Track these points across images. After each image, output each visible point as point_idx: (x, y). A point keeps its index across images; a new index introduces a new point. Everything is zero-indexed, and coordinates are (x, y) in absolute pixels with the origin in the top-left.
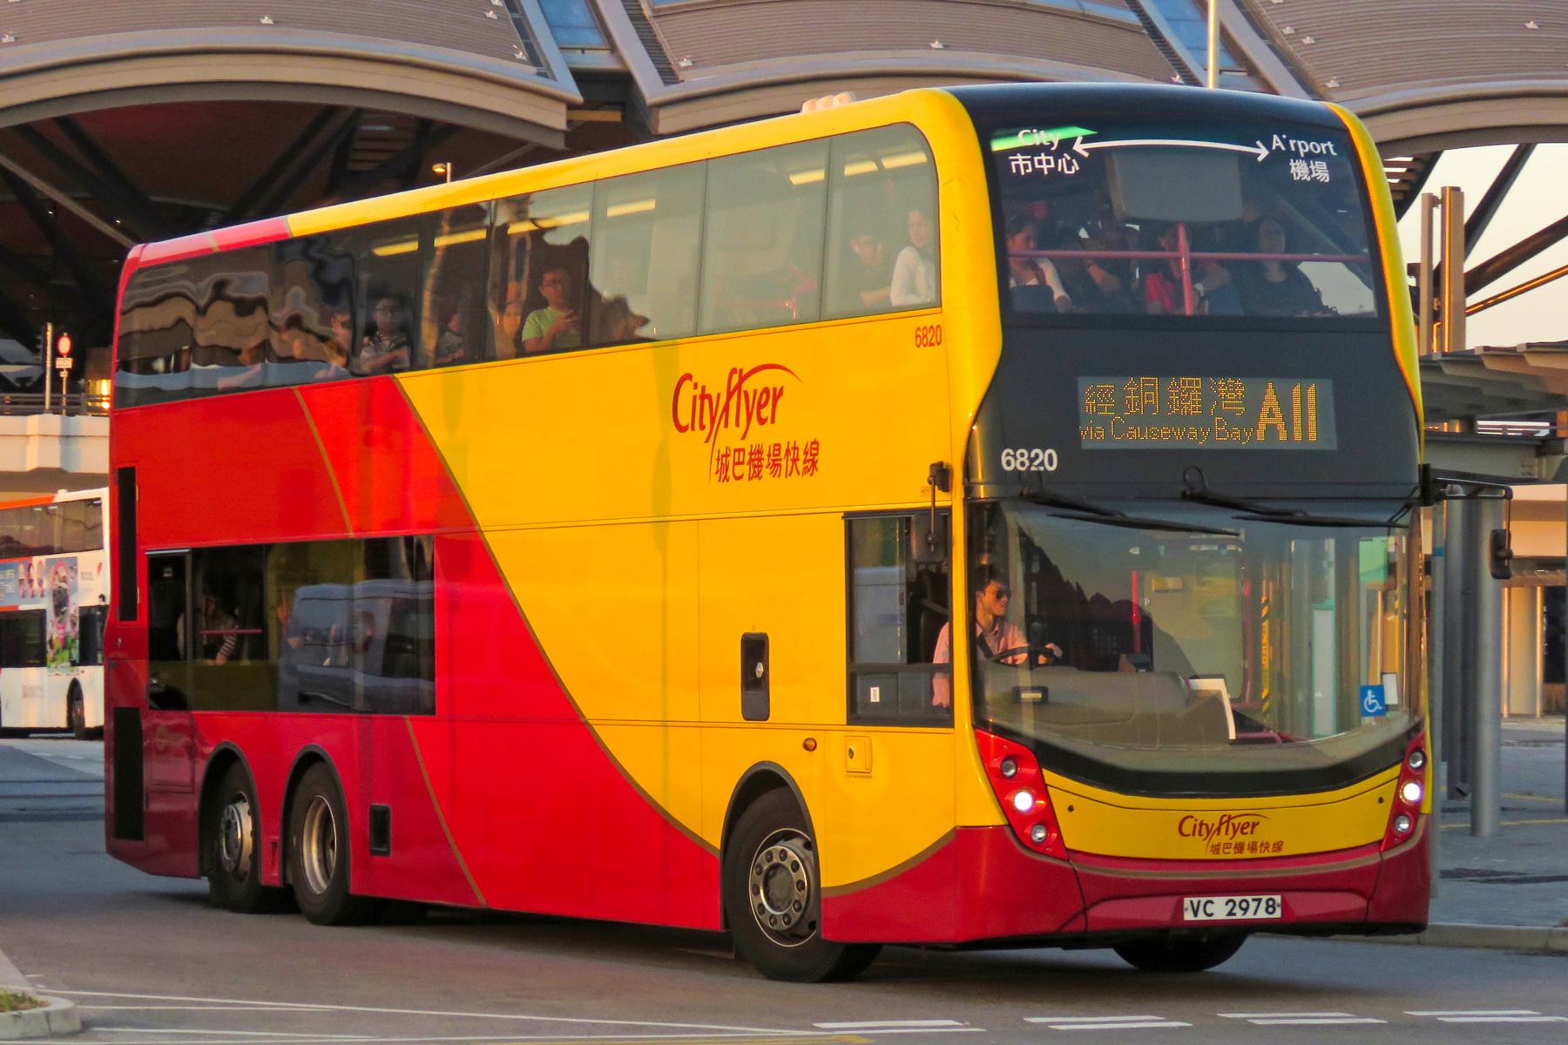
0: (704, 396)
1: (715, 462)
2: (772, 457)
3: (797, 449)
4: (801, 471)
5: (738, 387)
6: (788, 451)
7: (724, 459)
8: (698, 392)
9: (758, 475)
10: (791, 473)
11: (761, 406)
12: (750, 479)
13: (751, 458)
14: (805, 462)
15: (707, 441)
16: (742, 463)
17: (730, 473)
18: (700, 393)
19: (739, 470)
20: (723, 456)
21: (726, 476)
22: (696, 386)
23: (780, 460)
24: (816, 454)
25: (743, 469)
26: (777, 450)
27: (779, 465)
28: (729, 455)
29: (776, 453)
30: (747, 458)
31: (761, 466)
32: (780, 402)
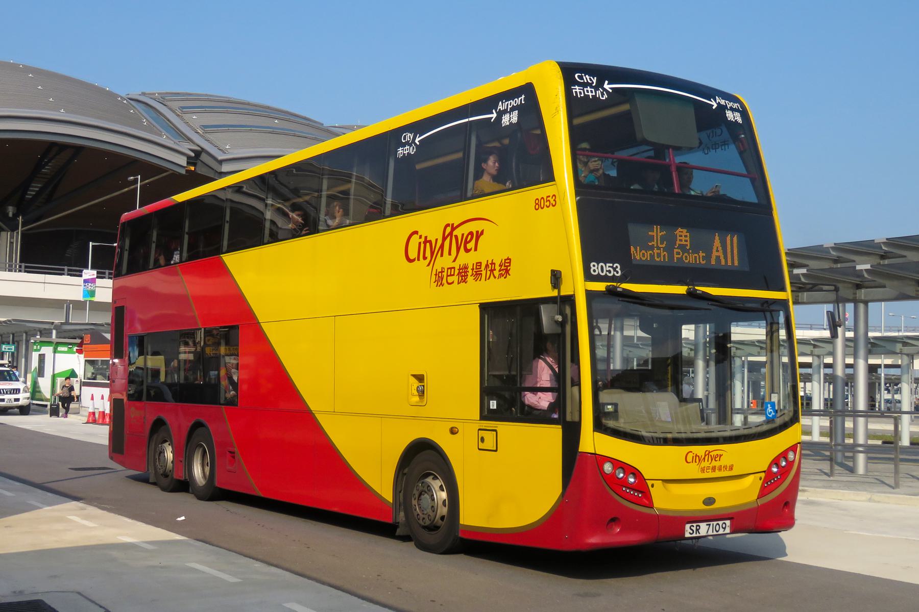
0: (426, 241)
1: (433, 277)
2: (475, 270)
3: (495, 264)
4: (497, 277)
5: (451, 234)
6: (487, 266)
7: (440, 274)
8: (423, 240)
9: (465, 281)
10: (489, 279)
11: (466, 242)
12: (458, 283)
13: (459, 271)
14: (500, 271)
15: (429, 265)
16: (454, 275)
17: (444, 281)
18: (424, 240)
19: (450, 279)
20: (439, 272)
21: (441, 283)
22: (421, 237)
23: (481, 271)
24: (510, 266)
25: (455, 278)
26: (479, 266)
27: (481, 274)
28: (444, 272)
29: (478, 267)
30: (457, 272)
31: (467, 275)
32: (482, 237)
